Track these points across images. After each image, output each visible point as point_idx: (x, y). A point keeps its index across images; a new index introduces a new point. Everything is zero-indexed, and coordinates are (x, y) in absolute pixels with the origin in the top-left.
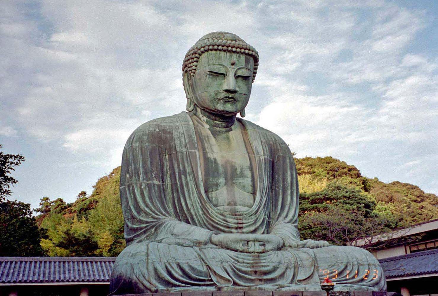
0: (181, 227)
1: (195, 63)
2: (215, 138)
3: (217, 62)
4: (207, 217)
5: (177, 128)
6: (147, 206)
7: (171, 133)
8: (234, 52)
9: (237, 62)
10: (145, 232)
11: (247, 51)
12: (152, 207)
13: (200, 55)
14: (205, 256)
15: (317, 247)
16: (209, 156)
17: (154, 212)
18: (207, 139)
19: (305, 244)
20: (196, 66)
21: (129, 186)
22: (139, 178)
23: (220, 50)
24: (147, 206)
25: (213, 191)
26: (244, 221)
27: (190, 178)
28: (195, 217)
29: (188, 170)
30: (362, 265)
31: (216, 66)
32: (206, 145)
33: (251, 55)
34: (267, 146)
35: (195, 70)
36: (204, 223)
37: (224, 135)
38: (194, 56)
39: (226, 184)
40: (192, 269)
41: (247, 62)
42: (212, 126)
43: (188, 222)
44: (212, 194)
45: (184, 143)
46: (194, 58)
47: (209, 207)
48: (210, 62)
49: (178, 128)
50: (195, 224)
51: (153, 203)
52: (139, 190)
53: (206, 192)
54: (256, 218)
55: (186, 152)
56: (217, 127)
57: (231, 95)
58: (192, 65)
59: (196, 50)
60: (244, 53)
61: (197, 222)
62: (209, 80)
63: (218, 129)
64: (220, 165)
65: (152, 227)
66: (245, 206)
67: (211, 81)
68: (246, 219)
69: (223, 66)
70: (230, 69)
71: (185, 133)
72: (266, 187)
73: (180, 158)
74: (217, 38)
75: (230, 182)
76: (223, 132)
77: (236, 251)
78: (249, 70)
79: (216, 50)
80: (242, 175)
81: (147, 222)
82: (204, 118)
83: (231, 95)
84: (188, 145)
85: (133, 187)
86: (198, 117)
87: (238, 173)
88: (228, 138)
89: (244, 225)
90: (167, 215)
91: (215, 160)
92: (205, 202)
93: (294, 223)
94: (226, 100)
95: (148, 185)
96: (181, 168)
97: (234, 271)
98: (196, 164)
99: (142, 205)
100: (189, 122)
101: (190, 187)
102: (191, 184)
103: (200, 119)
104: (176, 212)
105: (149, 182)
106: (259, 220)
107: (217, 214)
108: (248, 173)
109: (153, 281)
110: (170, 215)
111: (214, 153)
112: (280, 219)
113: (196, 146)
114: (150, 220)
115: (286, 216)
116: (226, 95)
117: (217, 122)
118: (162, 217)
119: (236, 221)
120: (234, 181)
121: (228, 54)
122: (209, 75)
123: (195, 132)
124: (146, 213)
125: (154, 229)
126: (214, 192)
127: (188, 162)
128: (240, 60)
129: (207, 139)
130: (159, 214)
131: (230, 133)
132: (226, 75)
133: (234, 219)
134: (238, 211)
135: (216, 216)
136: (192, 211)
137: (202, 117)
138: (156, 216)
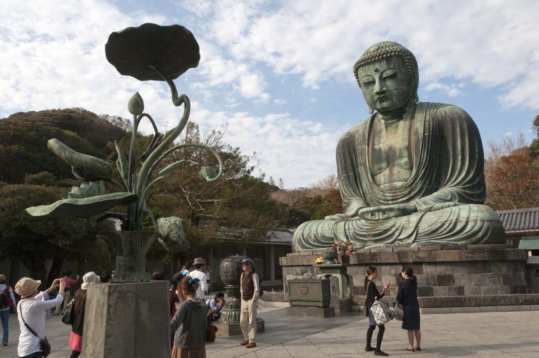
2: (386, 130)
6: (346, 192)
7: (354, 136)
8: (375, 61)
14: (336, 227)
15: (442, 208)
17: (349, 195)
19: (431, 208)
27: (363, 167)
29: (362, 162)
30: (462, 222)
33: (391, 56)
34: (431, 123)
37: (394, 126)
39: (388, 166)
40: (323, 237)
42: (386, 120)
51: (348, 190)
57: (382, 96)
64: (383, 153)
66: (402, 181)
68: (400, 192)
69: (369, 75)
72: (424, 161)
75: (391, 165)
77: (369, 220)
78: (392, 69)
79: (362, 66)
80: (401, 157)
83: (382, 96)
88: (397, 127)
91: (380, 149)
93: (463, 185)
97: (354, 236)
104: (363, 193)
108: (405, 153)
109: (297, 245)
110: (359, 196)
112: (449, 183)
115: (455, 181)
119: (391, 195)
122: (365, 85)
131: (401, 122)
133: (390, 193)
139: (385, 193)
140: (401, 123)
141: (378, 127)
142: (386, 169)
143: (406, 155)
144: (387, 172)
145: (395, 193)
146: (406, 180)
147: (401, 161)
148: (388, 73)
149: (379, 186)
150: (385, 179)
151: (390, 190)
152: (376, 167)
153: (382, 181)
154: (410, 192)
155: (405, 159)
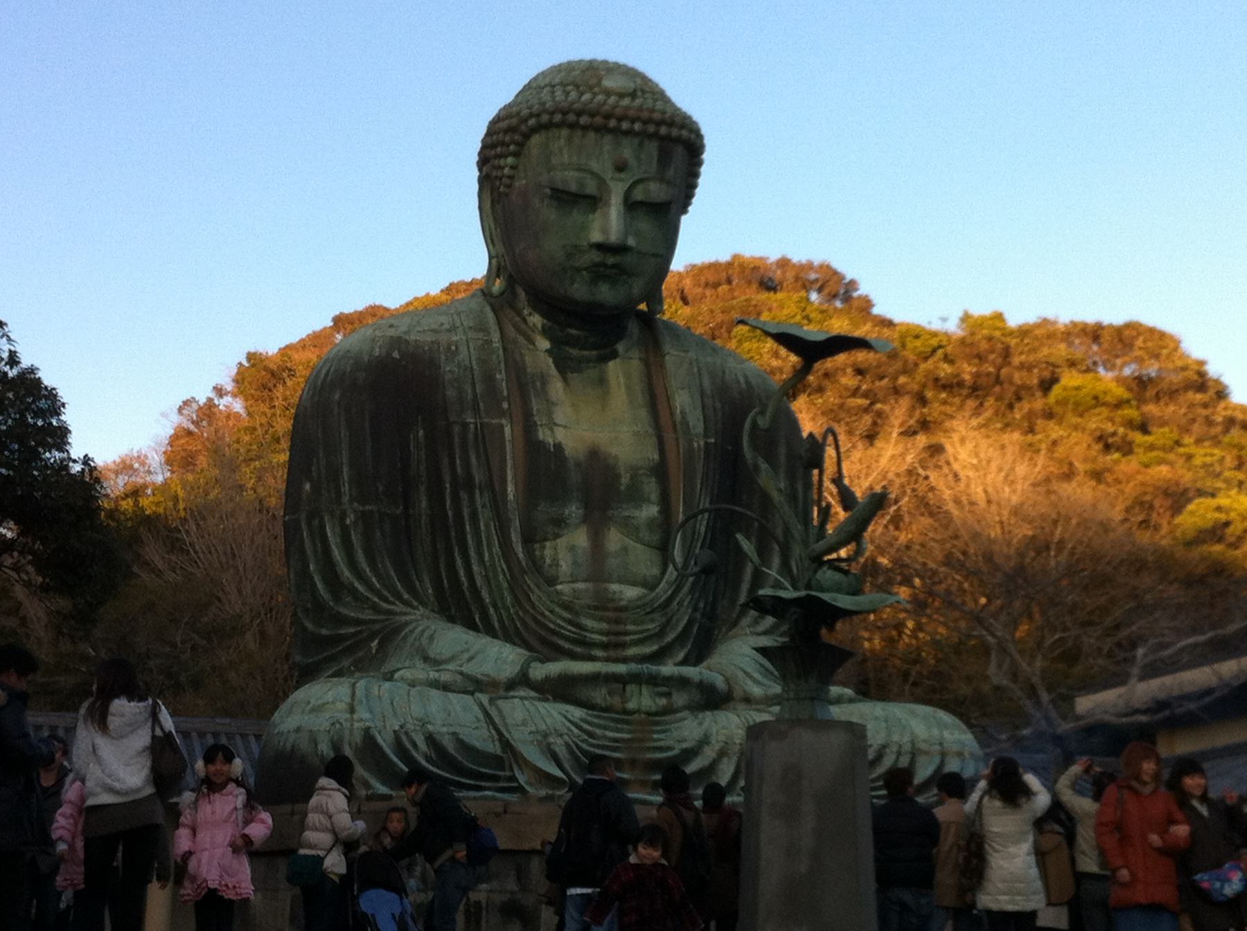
0: (451, 639)
1: (510, 160)
2: (565, 380)
3: (575, 159)
4: (526, 612)
5: (452, 352)
6: (360, 576)
8: (627, 133)
9: (632, 162)
10: (350, 650)
11: (663, 130)
12: (374, 580)
13: (527, 136)
16: (541, 437)
18: (538, 384)
20: (512, 167)
21: (311, 517)
22: (339, 494)
23: (585, 128)
24: (360, 576)
25: (546, 540)
26: (630, 628)
28: (492, 610)
29: (478, 476)
31: (571, 174)
32: (535, 405)
33: (678, 140)
35: (511, 177)
36: (517, 628)
38: (507, 139)
39: (585, 520)
41: (664, 158)
43: (472, 626)
44: (544, 547)
45: (470, 397)
46: (508, 146)
47: (532, 586)
48: (554, 161)
49: (457, 348)
50: (491, 632)
52: (338, 530)
53: (529, 539)
54: (664, 619)
55: (476, 424)
56: (574, 346)
57: (611, 260)
58: (502, 162)
59: (514, 121)
60: (655, 136)
61: (496, 625)
62: (549, 213)
63: (575, 352)
65: (372, 637)
66: (634, 584)
67: (553, 216)
68: (634, 623)
69: (592, 173)
70: (611, 184)
71: (475, 367)
73: (457, 439)
74: (577, 86)
76: (589, 361)
78: (669, 183)
79: (573, 126)
80: (635, 496)
81: (358, 622)
82: (536, 320)
83: (611, 260)
84: (481, 404)
85: (322, 519)
86: (519, 314)
87: (622, 488)
88: (602, 381)
89: (628, 638)
90: (415, 603)
91: (558, 447)
92: (525, 572)
94: (598, 273)
95: (364, 517)
96: (459, 470)
98: (503, 460)
99: (346, 573)
100: (489, 333)
101: (482, 524)
102: (485, 516)
103: (525, 320)
105: (368, 507)
106: (678, 621)
107: (553, 606)
108: (651, 488)
111: (555, 428)
113: (505, 405)
114: (368, 615)
116: (597, 259)
117: (573, 332)
118: (399, 607)
119: (604, 626)
120: (610, 513)
121: (608, 138)
122: (552, 197)
123: (506, 365)
124: (354, 593)
125: (375, 644)
126: (548, 544)
127: (477, 451)
128: (643, 156)
129: (538, 384)
130: (391, 599)
131: (611, 364)
132: (601, 199)
133: (601, 619)
134: (613, 600)
135: (551, 612)
136: (485, 594)
137: (530, 314)
138: (385, 605)
139: (577, 614)
140: (613, 366)
141: (528, 359)
142: (577, 526)
143: (654, 496)
144: (580, 538)
145: (618, 621)
146: (651, 585)
147: (637, 513)
148: (656, 191)
149: (552, 581)
150: (575, 563)
151: (596, 608)
152: (544, 510)
153: (565, 567)
154: (661, 633)
155: (651, 511)
